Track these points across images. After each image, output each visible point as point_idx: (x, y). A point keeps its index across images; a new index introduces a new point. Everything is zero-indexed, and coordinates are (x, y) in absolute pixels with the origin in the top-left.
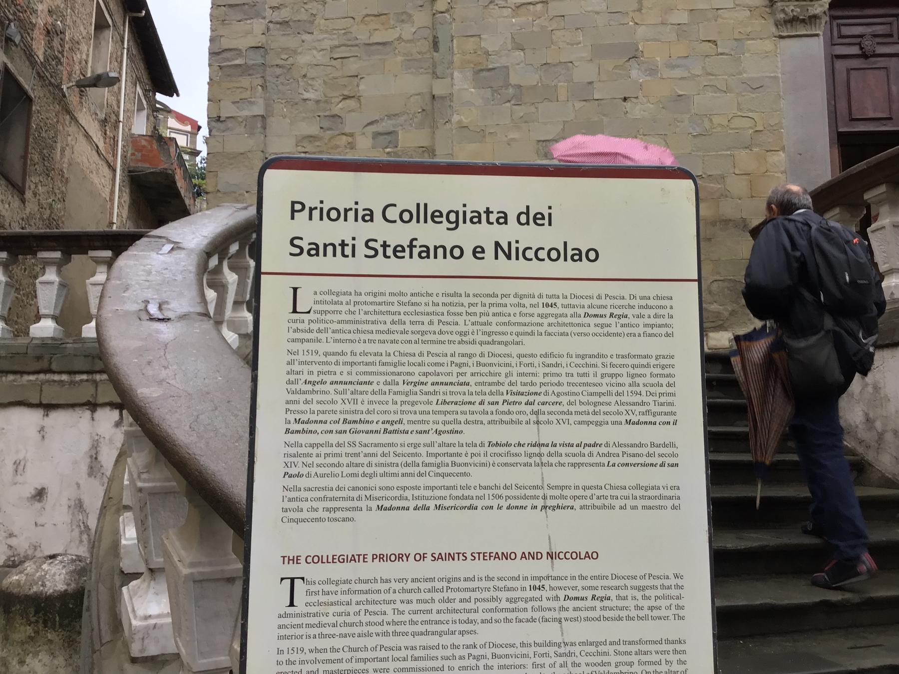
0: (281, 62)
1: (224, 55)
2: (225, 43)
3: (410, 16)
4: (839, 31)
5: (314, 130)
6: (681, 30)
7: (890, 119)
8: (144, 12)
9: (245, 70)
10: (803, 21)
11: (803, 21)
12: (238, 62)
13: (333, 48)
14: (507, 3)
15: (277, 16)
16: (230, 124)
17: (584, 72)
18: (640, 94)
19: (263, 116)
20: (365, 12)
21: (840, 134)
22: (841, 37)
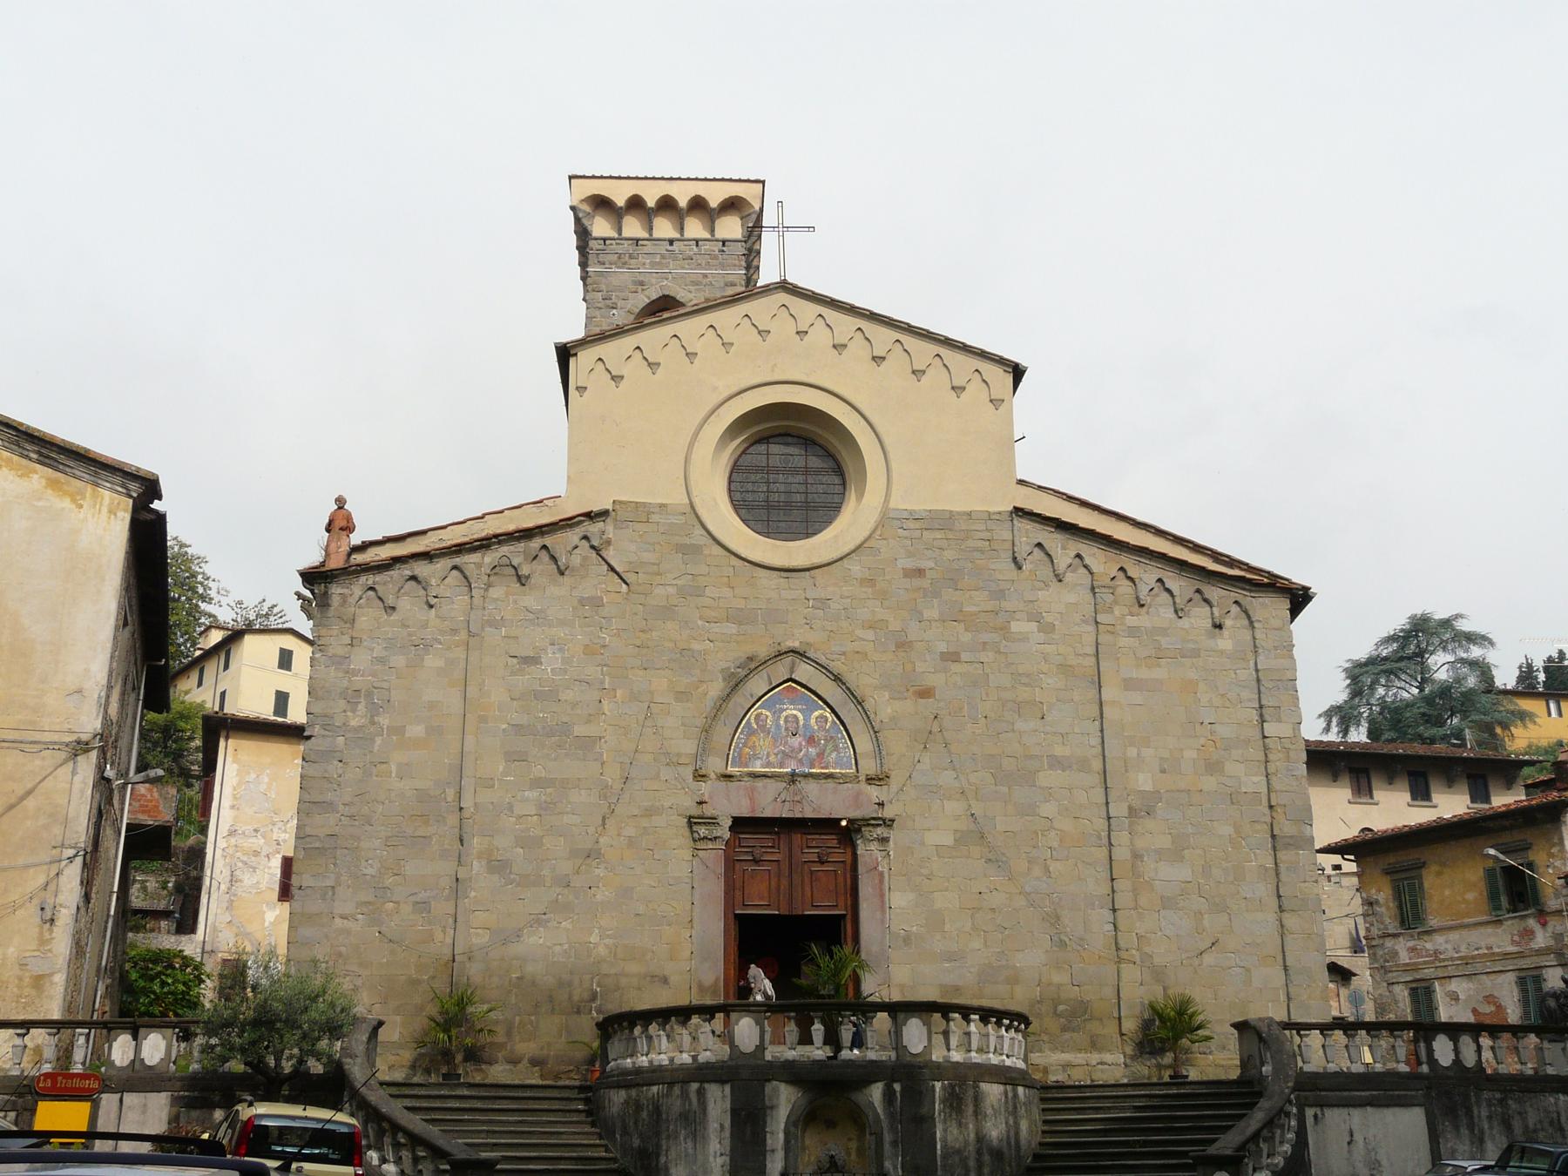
0: (349, 846)
1: (308, 839)
2: (308, 830)
3: (444, 817)
4: (740, 843)
5: (371, 898)
6: (631, 842)
7: (769, 905)
8: (164, 660)
9: (321, 851)
10: (710, 839)
11: (710, 839)
12: (317, 845)
13: (388, 838)
14: (513, 813)
15: (347, 810)
16: (309, 891)
17: (566, 867)
18: (601, 885)
19: (333, 887)
20: (412, 813)
21: (737, 916)
22: (740, 846)
